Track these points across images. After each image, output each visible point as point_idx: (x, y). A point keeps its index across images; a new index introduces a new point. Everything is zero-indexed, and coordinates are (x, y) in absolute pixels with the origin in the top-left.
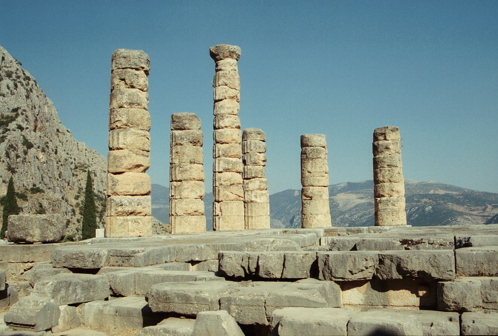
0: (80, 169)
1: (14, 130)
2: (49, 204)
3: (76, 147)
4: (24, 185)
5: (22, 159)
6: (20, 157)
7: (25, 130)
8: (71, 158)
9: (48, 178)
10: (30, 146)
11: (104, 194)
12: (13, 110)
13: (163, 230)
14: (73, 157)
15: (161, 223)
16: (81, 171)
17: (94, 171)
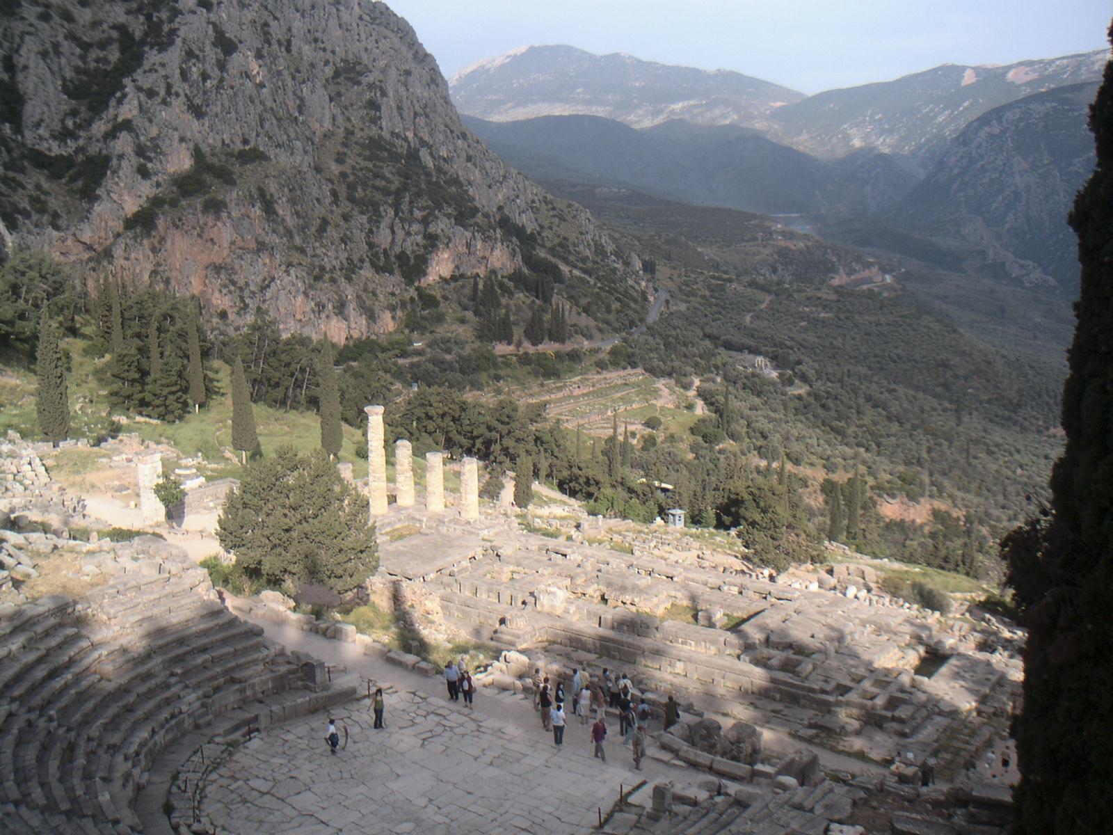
0: (347, 79)
1: (194, 12)
2: (282, 186)
3: (336, 22)
4: (223, 141)
5: (215, 82)
6: (209, 77)
7: (215, 8)
8: (324, 50)
9: (274, 121)
10: (227, 46)
11: (406, 139)
13: (554, 216)
14: (329, 48)
15: (550, 197)
16: (349, 84)
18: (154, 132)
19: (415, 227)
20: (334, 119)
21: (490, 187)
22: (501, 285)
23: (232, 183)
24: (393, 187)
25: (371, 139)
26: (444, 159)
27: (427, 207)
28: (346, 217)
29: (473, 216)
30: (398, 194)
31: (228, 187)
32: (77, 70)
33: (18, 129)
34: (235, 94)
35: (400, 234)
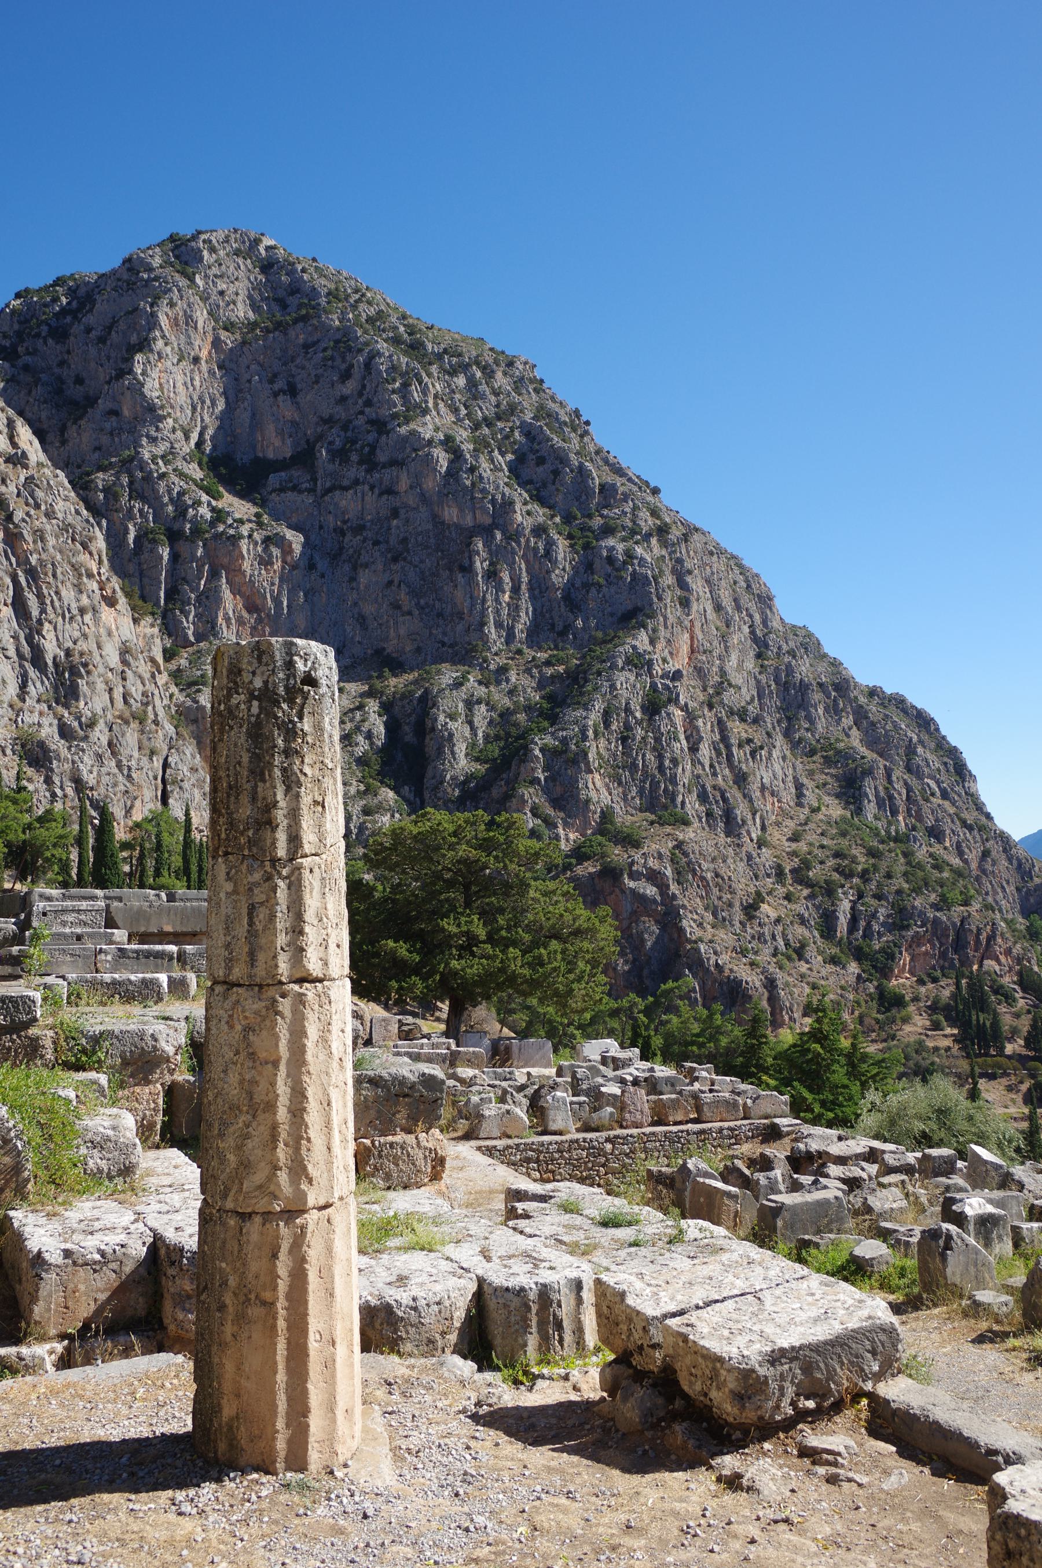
12: (623, 615)
17: (863, 758)
18: (559, 790)
19: (882, 911)
20: (800, 795)
21: (1018, 889)
22: (998, 990)
23: (637, 845)
24: (860, 868)
25: (843, 818)
26: (945, 848)
27: (899, 892)
28: (788, 897)
29: (966, 903)
30: (865, 872)
31: (632, 852)
32: (486, 737)
33: (419, 792)
34: (660, 757)
35: (862, 923)
